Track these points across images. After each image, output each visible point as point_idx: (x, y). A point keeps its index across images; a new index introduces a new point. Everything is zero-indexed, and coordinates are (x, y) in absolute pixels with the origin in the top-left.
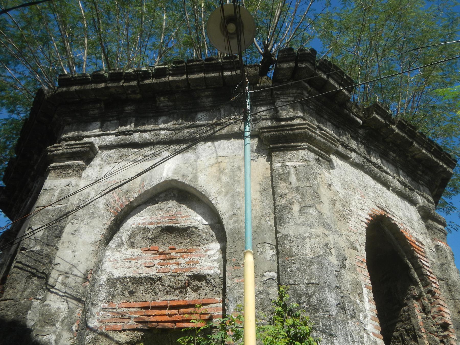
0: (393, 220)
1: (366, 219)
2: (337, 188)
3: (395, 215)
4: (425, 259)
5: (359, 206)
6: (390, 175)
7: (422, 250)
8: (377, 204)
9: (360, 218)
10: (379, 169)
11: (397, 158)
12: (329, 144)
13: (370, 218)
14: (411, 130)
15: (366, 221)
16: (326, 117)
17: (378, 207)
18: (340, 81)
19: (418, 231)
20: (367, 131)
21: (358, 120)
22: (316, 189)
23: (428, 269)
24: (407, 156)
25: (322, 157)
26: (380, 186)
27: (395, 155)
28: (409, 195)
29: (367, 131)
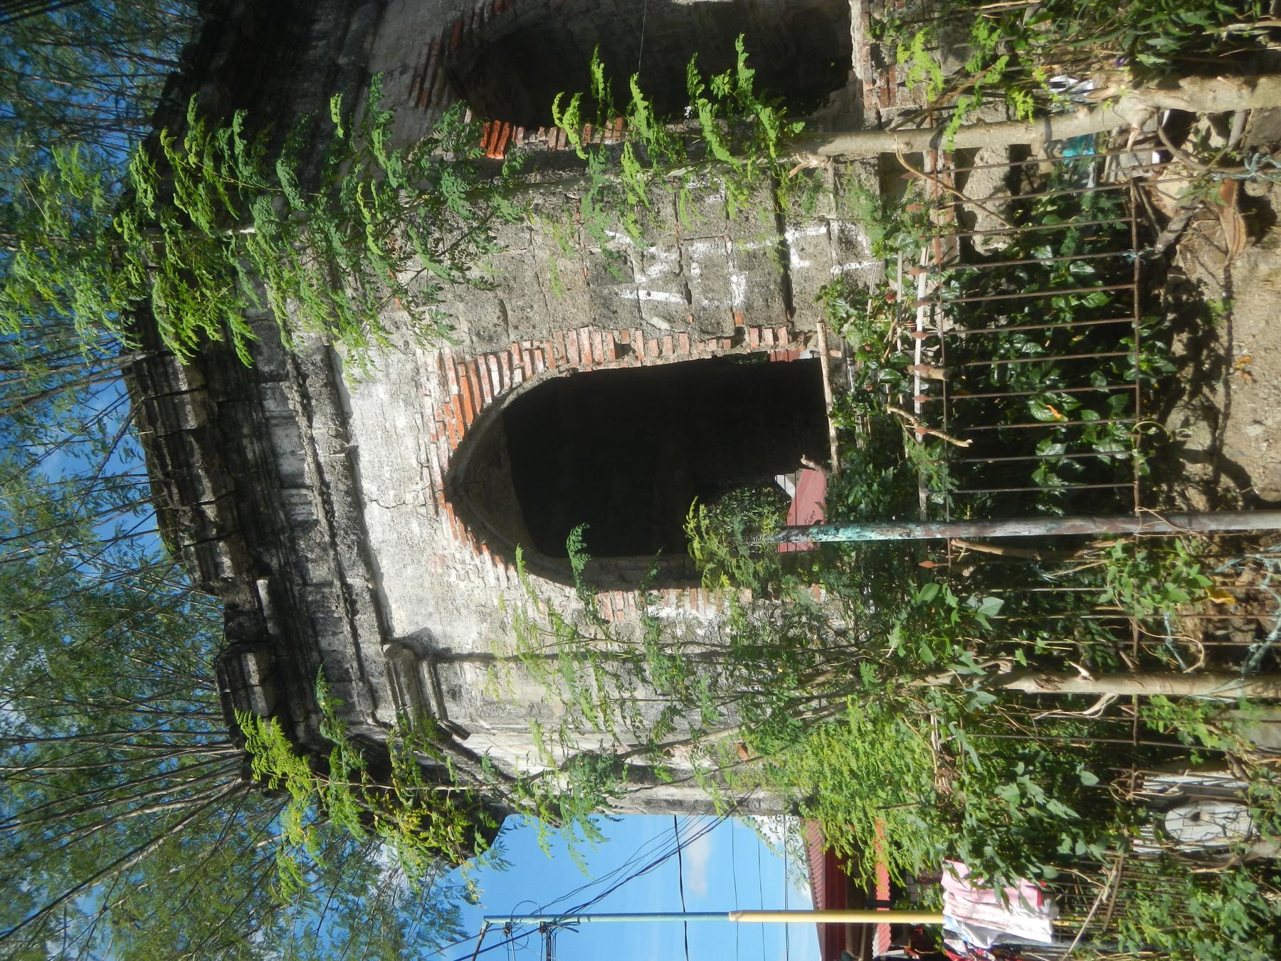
0: (442, 472)
1: (495, 565)
2: (474, 636)
3: (423, 457)
4: (483, 369)
5: (478, 581)
6: (315, 455)
7: (461, 369)
8: (432, 511)
9: (504, 584)
10: (329, 495)
11: (246, 431)
12: (402, 679)
13: (486, 554)
14: (172, 459)
15: (501, 567)
16: (315, 655)
17: (437, 512)
18: (242, 693)
19: (409, 366)
20: (260, 549)
21: (263, 593)
22: (523, 711)
23: (506, 372)
24: (220, 405)
25: (439, 684)
26: (368, 486)
27: (246, 442)
28: (325, 385)
29: (260, 549)
